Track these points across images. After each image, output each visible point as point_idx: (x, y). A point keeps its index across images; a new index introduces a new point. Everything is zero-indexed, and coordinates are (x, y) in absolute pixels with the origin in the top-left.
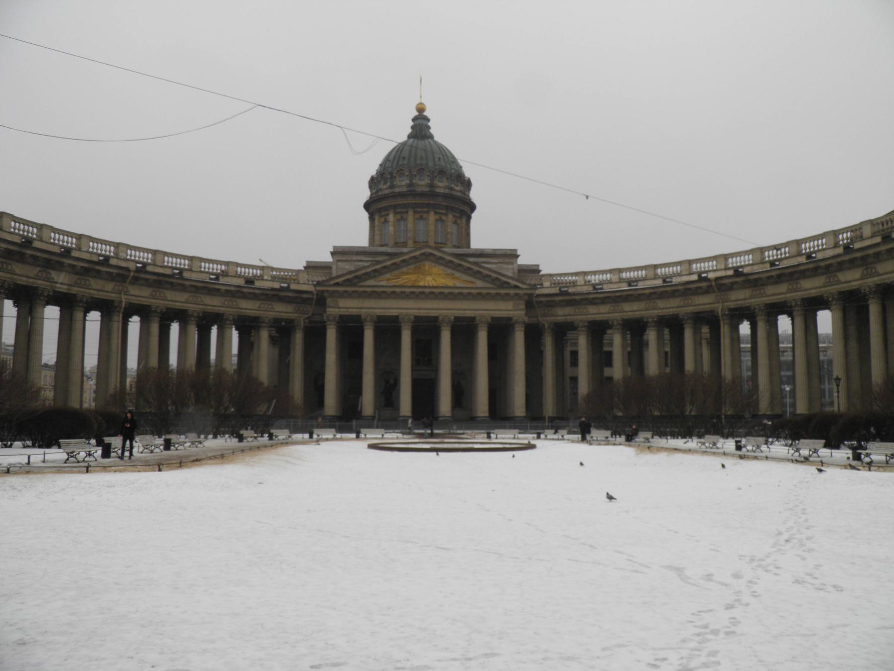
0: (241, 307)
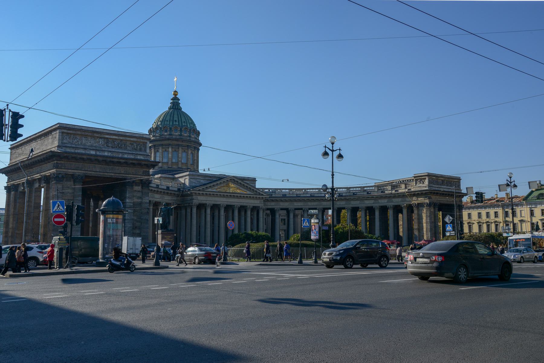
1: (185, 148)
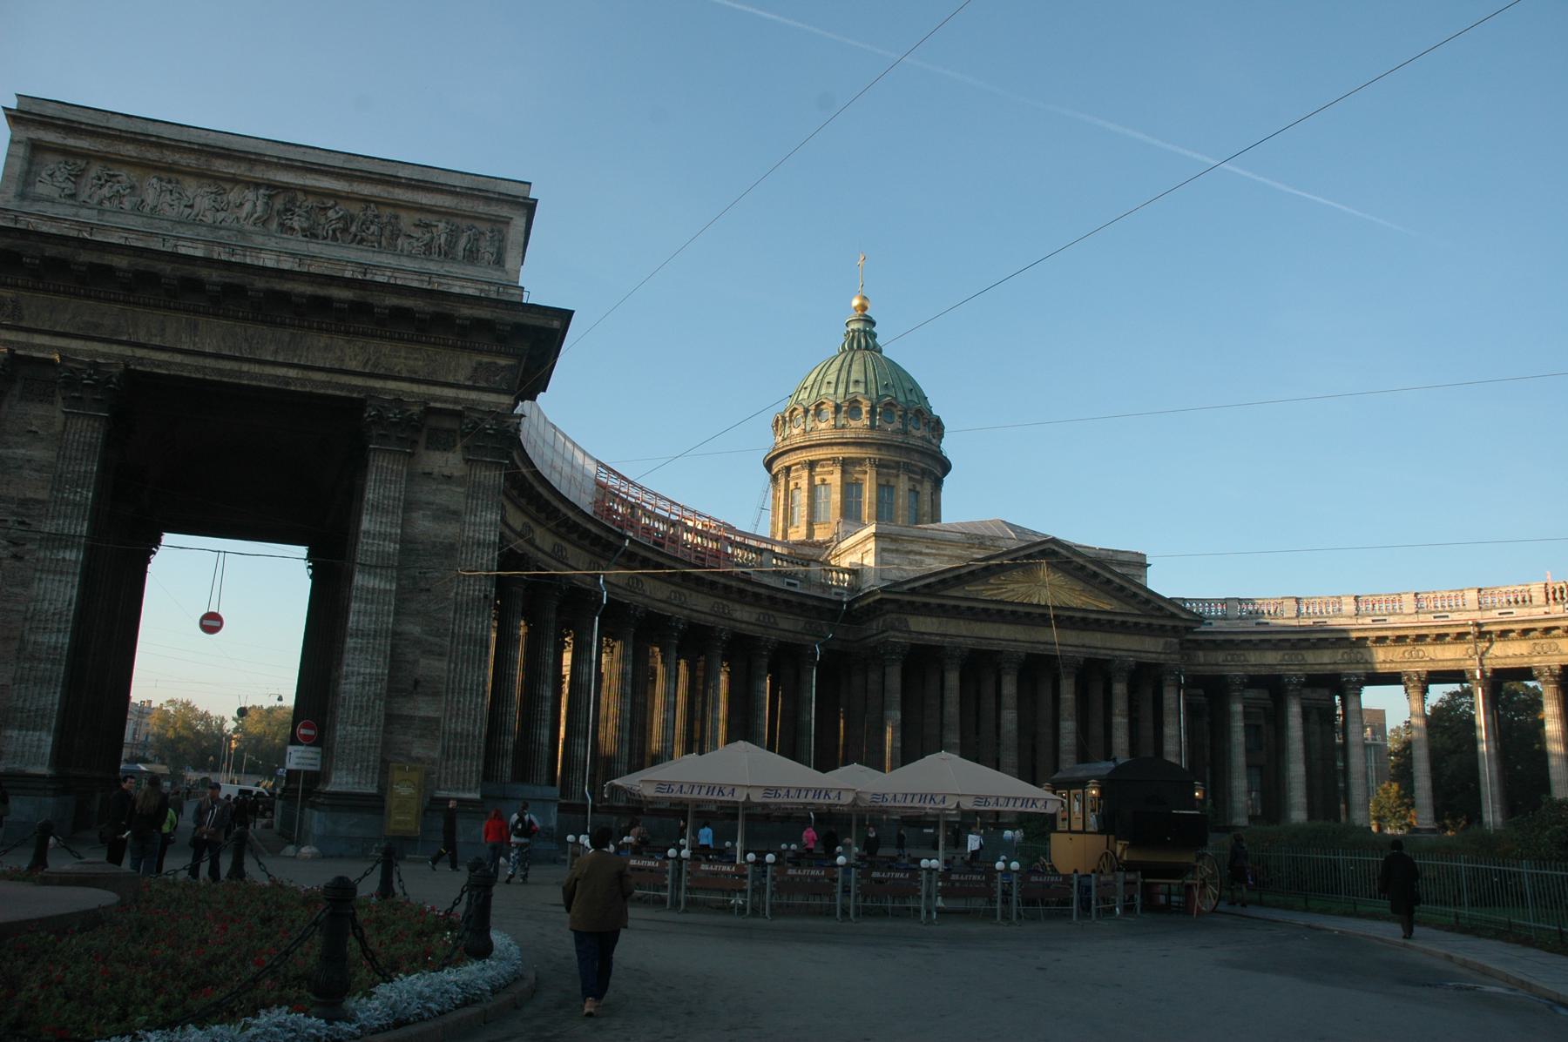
1: (891, 471)
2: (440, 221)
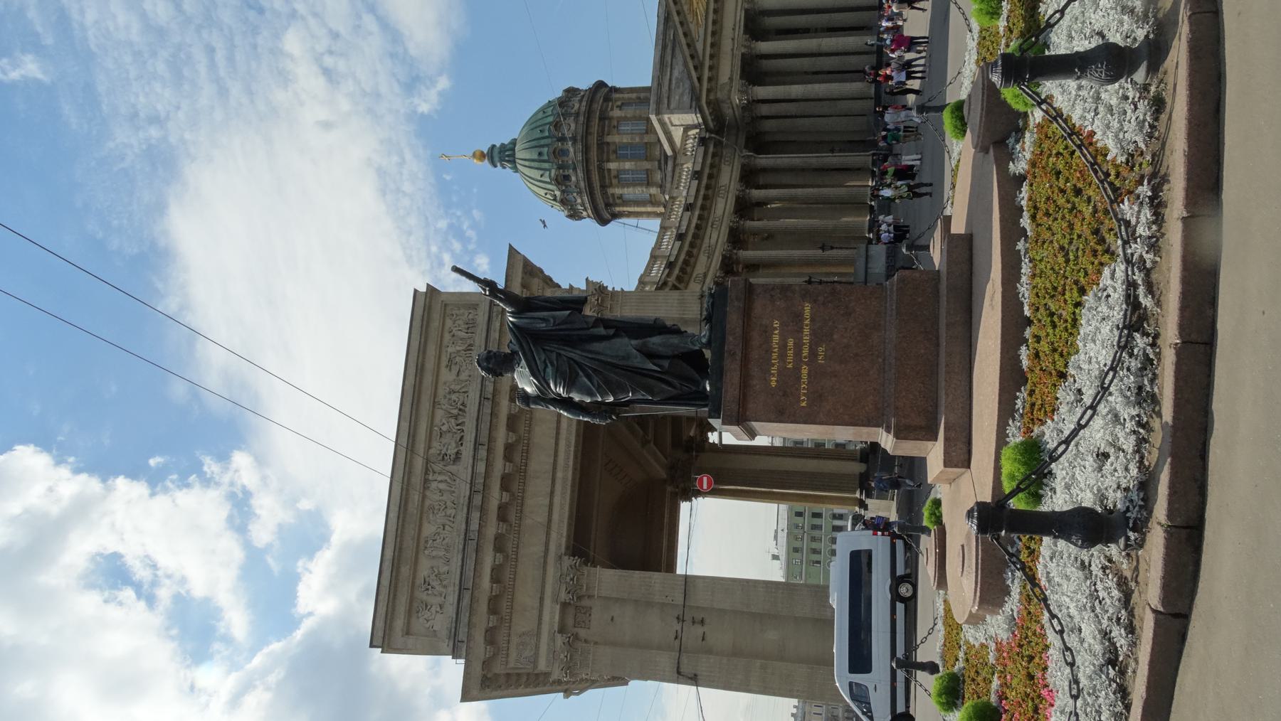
0: (722, 214)
2: (447, 351)
